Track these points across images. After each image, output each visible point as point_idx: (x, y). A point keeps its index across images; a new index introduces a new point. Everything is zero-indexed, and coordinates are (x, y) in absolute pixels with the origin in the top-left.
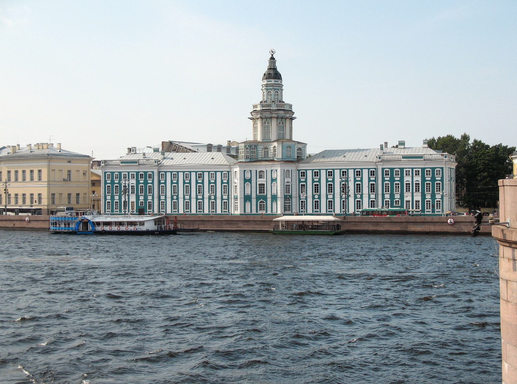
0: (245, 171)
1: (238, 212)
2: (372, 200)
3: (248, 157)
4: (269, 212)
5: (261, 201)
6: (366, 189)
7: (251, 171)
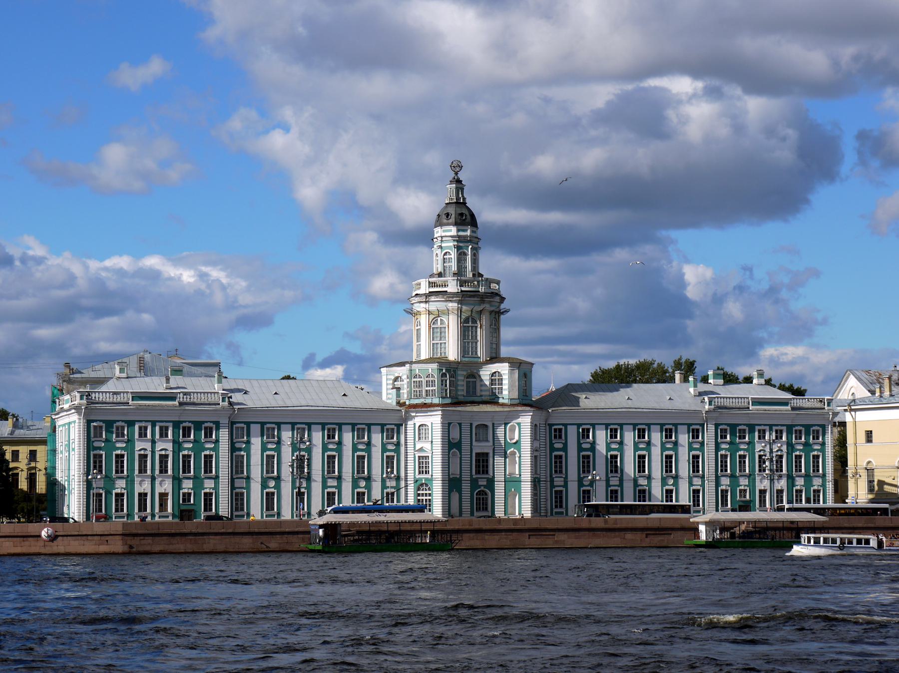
0: (449, 424)
2: (694, 487)
3: (446, 394)
7: (460, 424)
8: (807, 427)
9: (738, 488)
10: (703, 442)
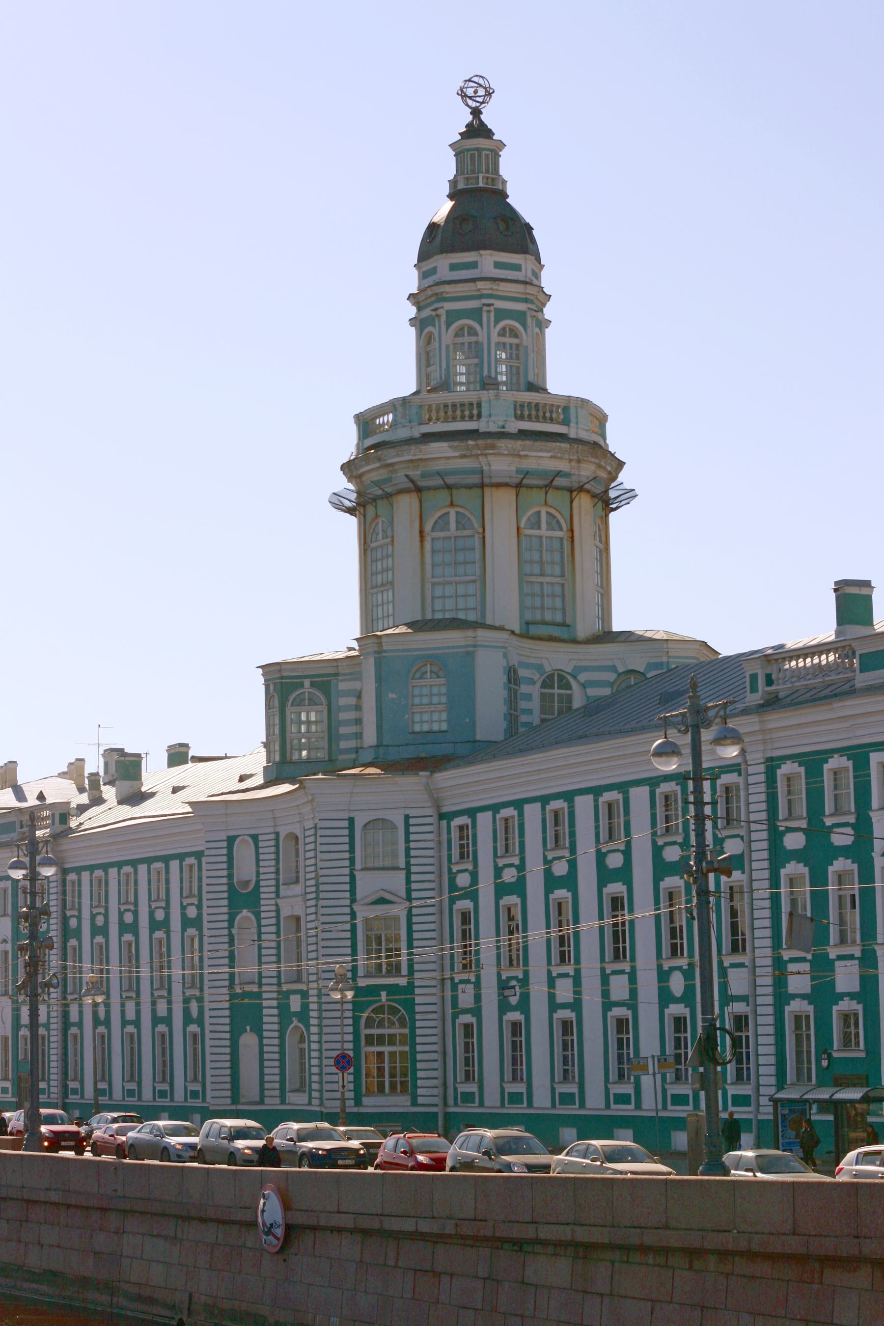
0: (231, 840)
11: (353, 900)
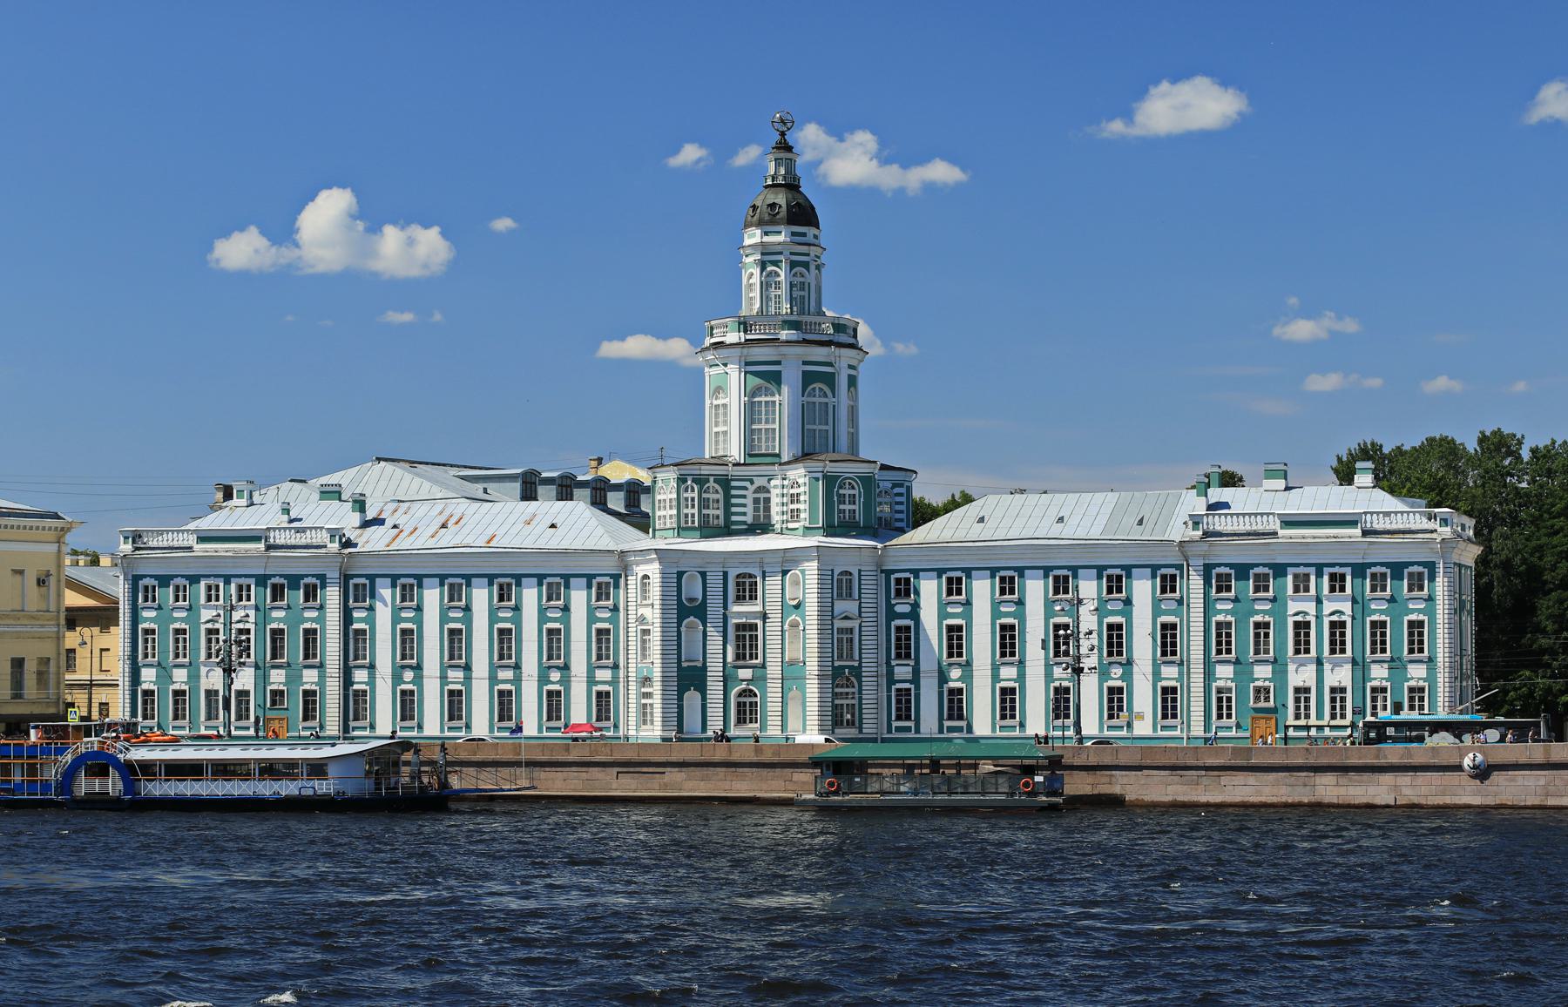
0: (680, 574)
1: (654, 732)
4: (774, 730)
5: (744, 691)
6: (1143, 645)
7: (703, 575)
8: (1397, 569)
9: (1252, 685)
10: (1182, 597)
11: (833, 615)
